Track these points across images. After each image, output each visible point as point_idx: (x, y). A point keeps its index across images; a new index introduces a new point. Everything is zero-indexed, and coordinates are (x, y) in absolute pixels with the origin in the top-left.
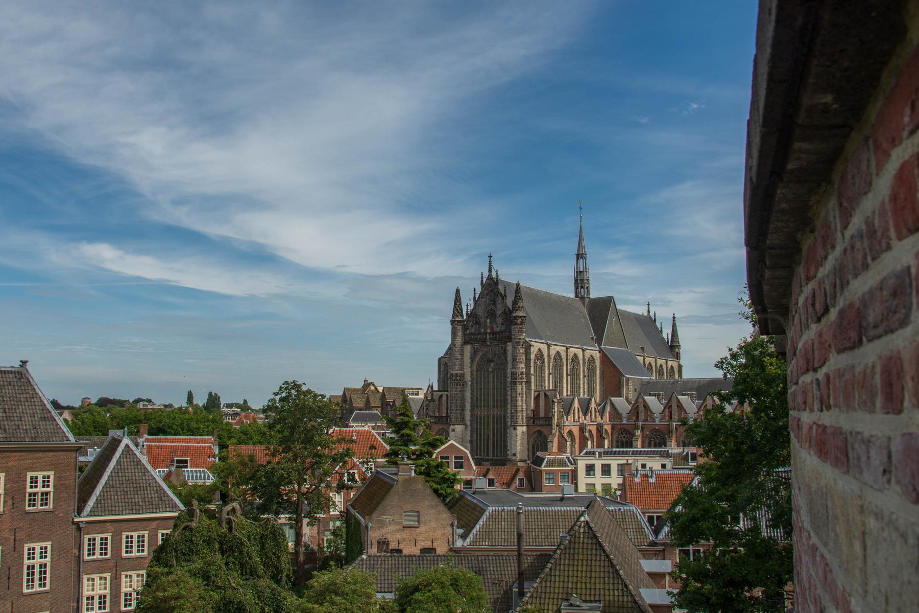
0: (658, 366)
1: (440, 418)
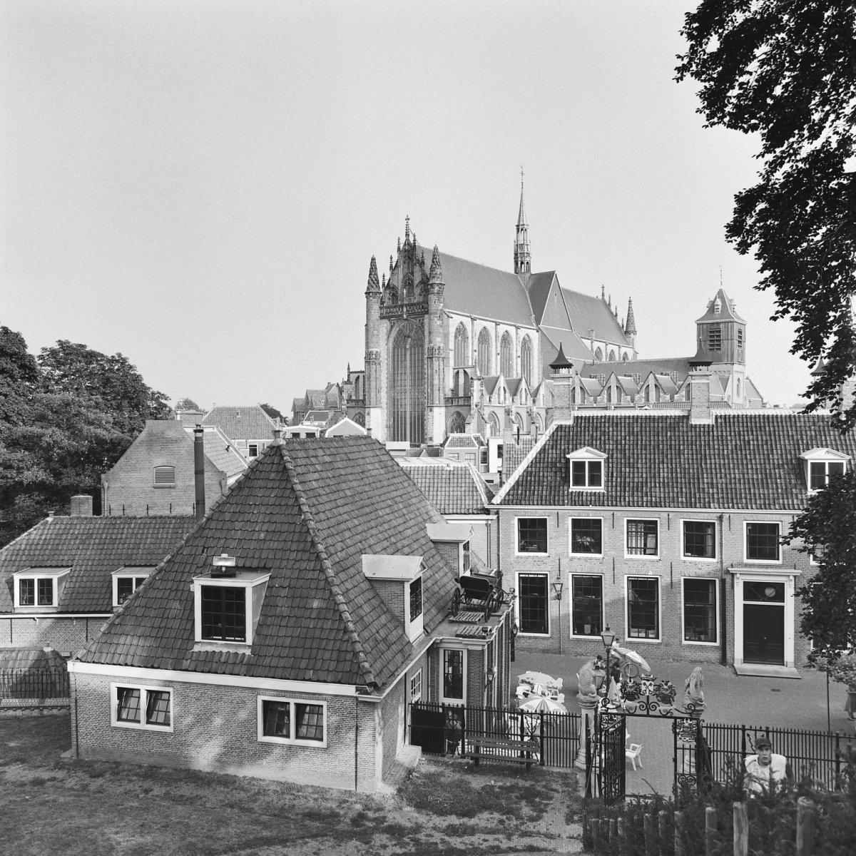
0: (609, 352)
1: (357, 401)
